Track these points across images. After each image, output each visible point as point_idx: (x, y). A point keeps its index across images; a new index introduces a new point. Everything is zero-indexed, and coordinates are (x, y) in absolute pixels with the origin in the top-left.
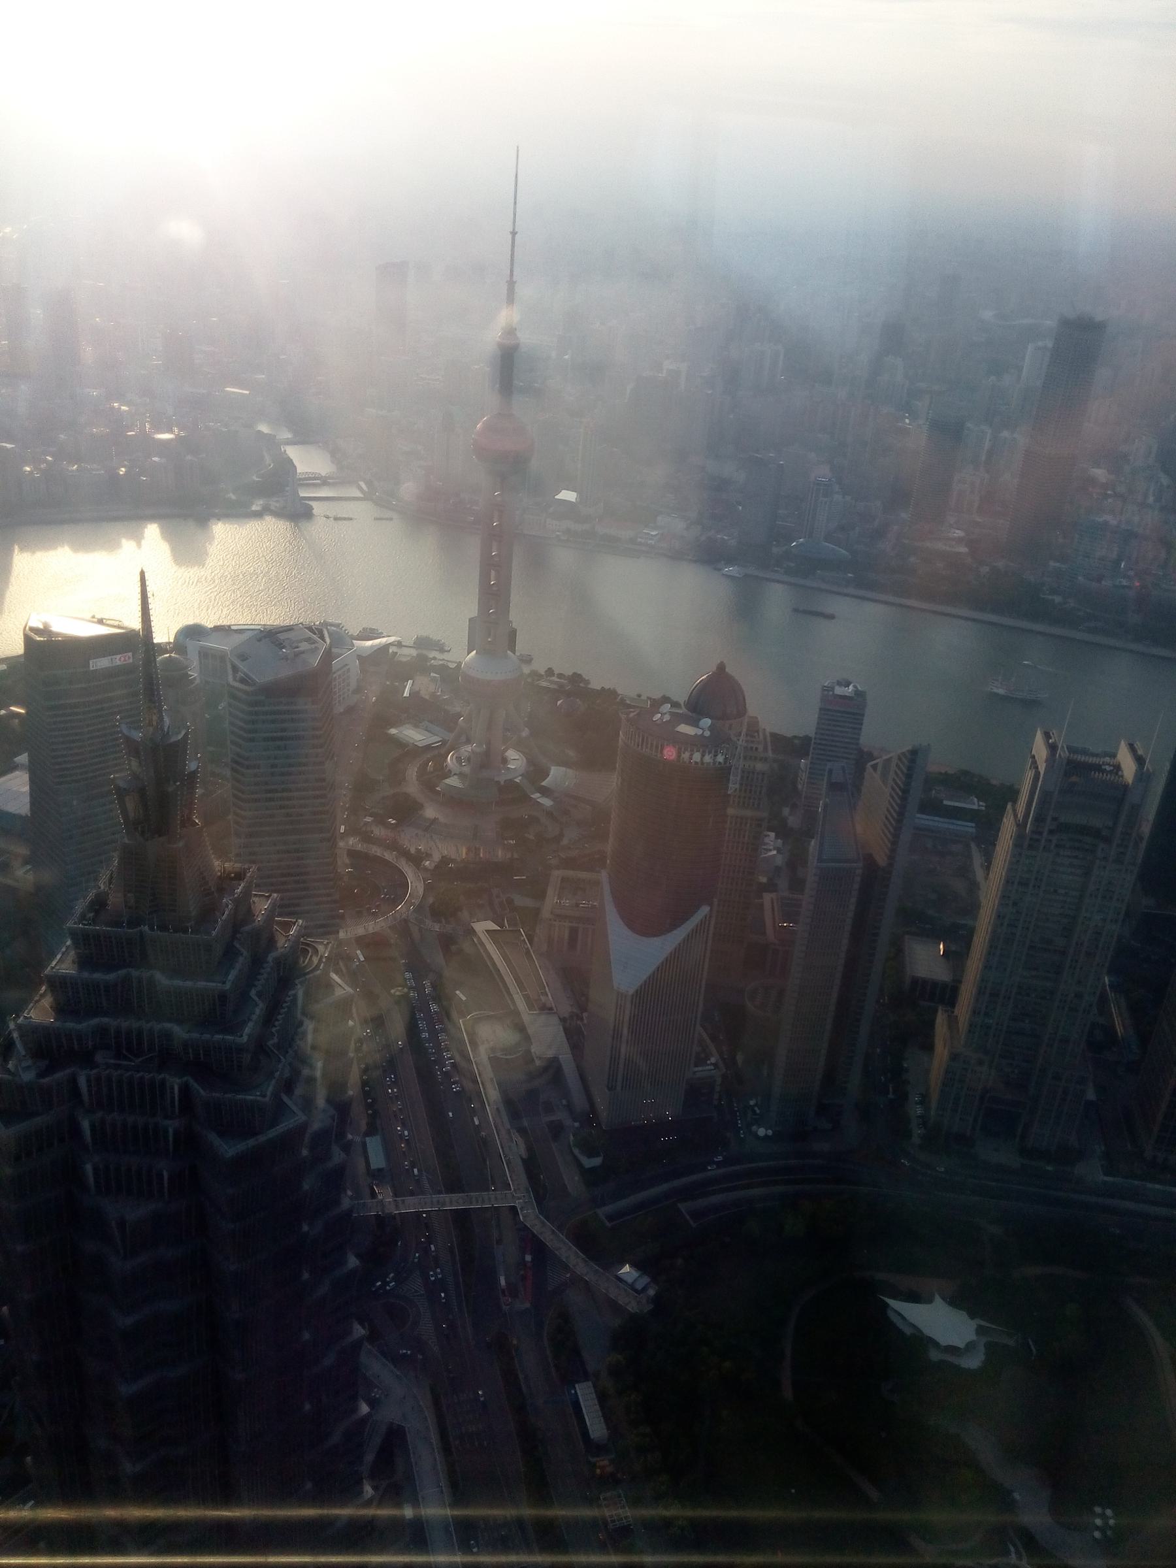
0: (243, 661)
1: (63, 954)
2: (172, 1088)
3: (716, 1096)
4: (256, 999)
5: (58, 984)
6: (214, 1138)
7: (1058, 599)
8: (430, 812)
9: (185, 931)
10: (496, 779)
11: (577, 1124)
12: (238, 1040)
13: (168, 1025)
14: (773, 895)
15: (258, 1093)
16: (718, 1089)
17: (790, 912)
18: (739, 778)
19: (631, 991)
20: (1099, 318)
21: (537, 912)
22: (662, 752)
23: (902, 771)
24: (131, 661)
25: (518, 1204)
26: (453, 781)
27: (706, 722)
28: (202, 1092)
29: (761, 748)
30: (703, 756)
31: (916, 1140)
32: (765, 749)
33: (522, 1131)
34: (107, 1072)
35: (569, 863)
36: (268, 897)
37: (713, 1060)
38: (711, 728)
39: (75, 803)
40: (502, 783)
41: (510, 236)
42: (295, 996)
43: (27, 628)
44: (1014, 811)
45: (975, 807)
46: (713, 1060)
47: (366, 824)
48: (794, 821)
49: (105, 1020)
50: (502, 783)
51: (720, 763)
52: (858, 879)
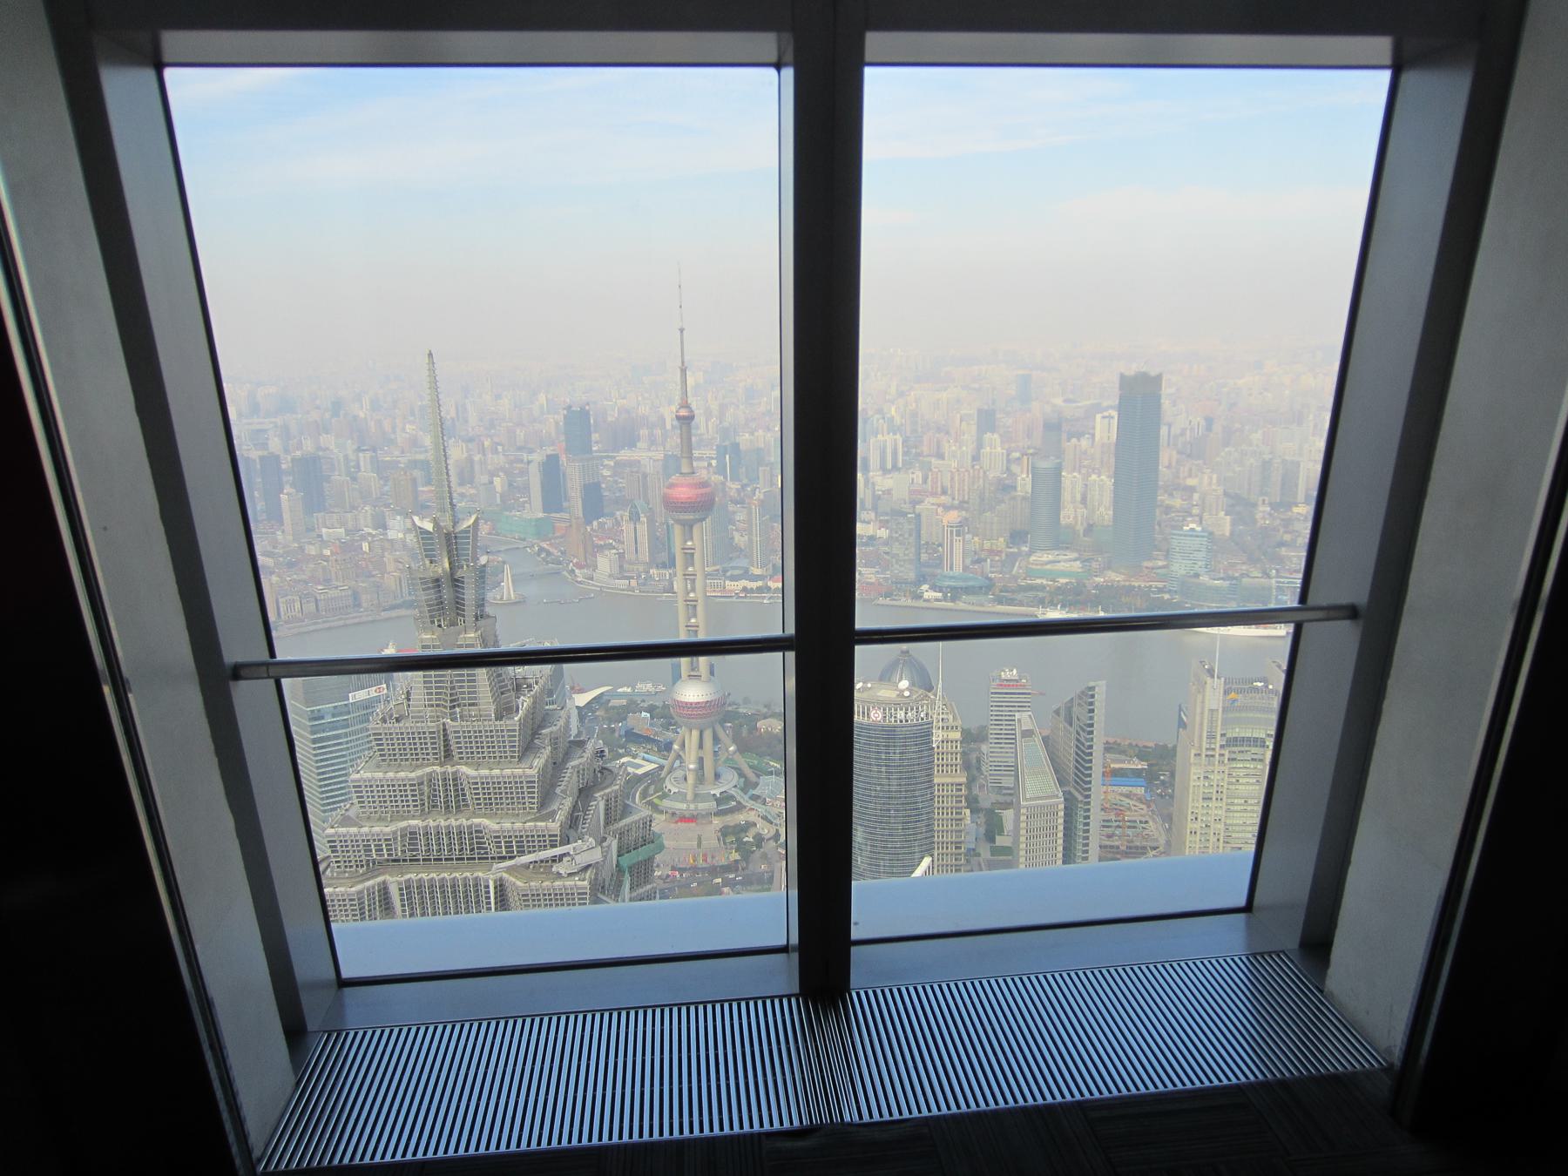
2: (487, 887)
7: (1167, 596)
10: (712, 792)
13: (476, 821)
15: (577, 878)
20: (1153, 373)
28: (519, 883)
29: (951, 717)
30: (906, 713)
40: (718, 795)
41: (679, 332)
45: (1140, 767)
48: (987, 799)
50: (718, 795)
51: (922, 719)
52: (1061, 814)
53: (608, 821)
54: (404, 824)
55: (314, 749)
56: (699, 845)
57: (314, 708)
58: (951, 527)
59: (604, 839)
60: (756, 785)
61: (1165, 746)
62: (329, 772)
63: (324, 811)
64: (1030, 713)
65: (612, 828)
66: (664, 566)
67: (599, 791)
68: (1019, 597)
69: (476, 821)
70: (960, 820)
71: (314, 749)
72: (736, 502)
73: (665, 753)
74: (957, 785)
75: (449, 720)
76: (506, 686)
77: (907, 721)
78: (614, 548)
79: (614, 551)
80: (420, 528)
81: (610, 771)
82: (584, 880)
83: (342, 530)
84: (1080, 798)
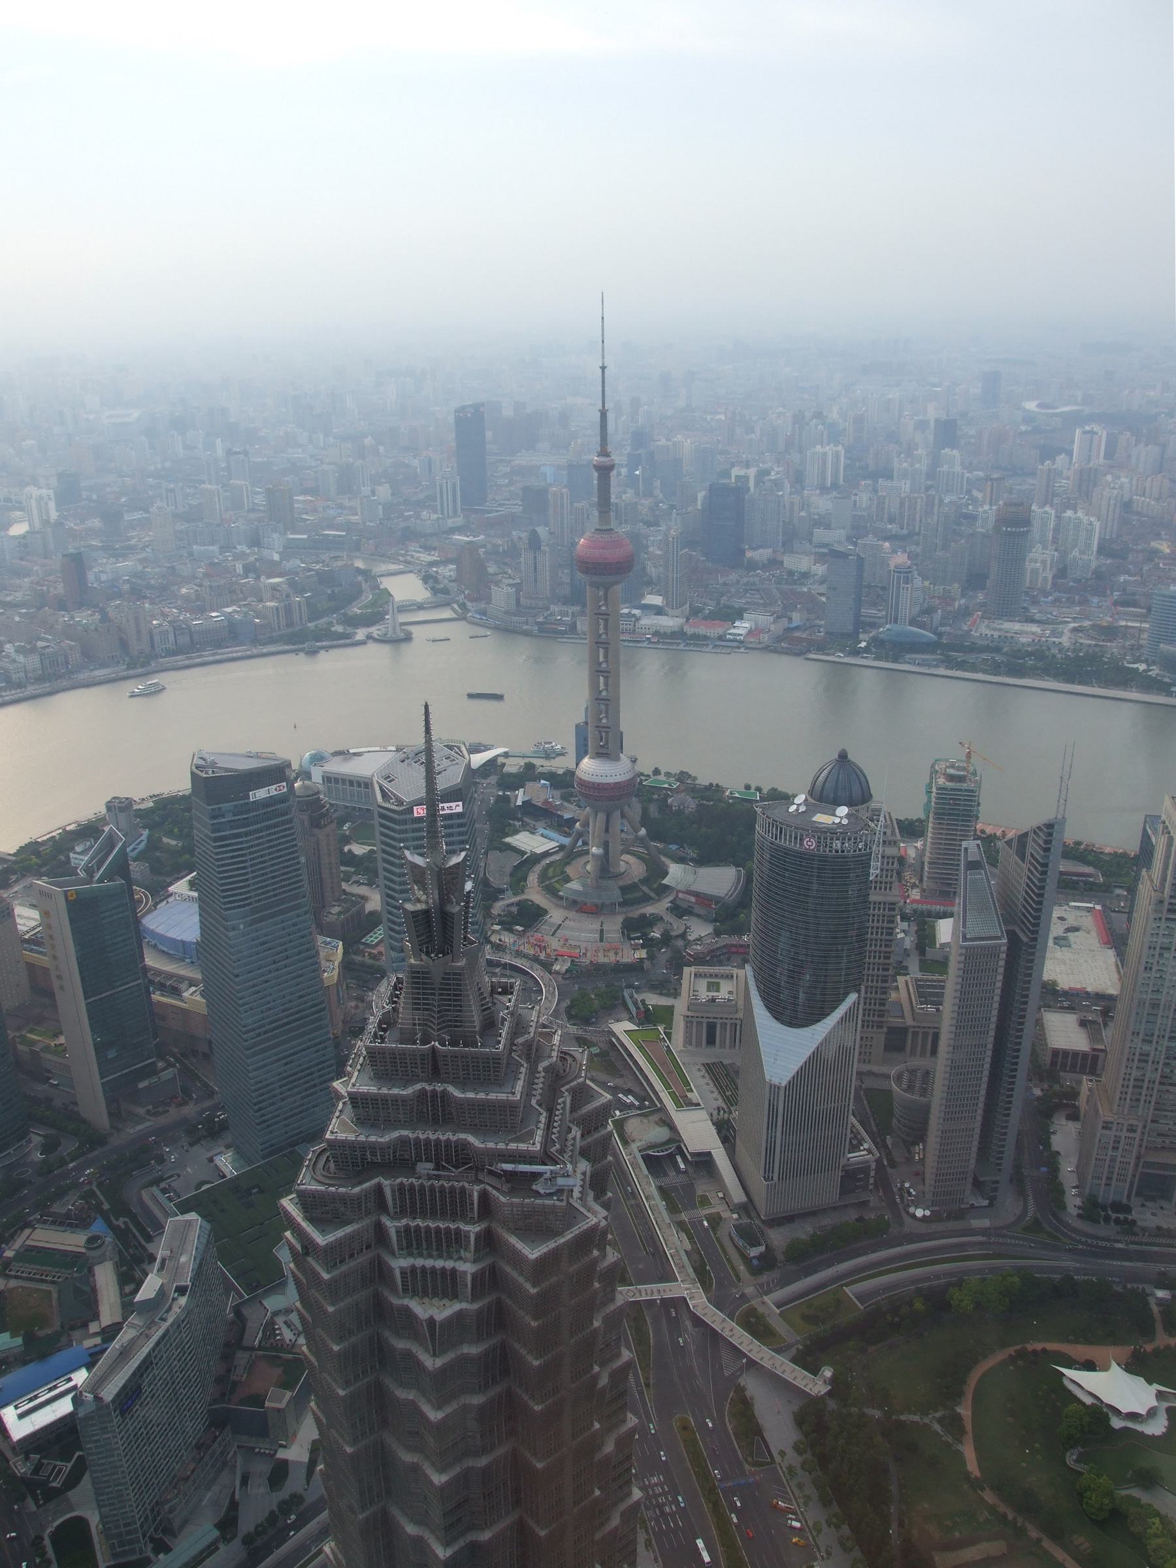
0: (390, 782)
1: (359, 1071)
2: (471, 1196)
3: (872, 1181)
4: (537, 1107)
5: (356, 1100)
6: (513, 1240)
8: (556, 915)
9: (474, 1045)
11: (735, 1216)
12: (531, 1148)
13: (462, 1136)
14: (908, 978)
15: (555, 1198)
16: (873, 1173)
17: (929, 994)
18: (879, 864)
19: (784, 1084)
21: (670, 1010)
22: (801, 844)
23: (1039, 845)
24: (285, 790)
25: (685, 1294)
26: (574, 885)
27: (843, 811)
28: (502, 1199)
30: (843, 843)
31: (1074, 1212)
32: (893, 833)
33: (681, 1226)
34: (430, 1182)
35: (699, 960)
36: (533, 1007)
37: (866, 1146)
38: (848, 816)
39: (242, 927)
42: (564, 1103)
43: (194, 767)
44: (1150, 877)
46: (866, 1146)
47: (494, 931)
49: (405, 1133)
51: (860, 850)
52: (1003, 956)
53: (573, 1110)
54: (395, 1134)
55: (216, 847)
56: (601, 940)
57: (216, 806)
58: (898, 572)
59: (569, 1130)
60: (665, 874)
61: (1124, 855)
62: (228, 858)
63: (226, 909)
64: (979, 842)
65: (576, 1115)
66: (566, 601)
67: (563, 1086)
68: (971, 658)
69: (462, 1136)
70: (891, 941)
71: (216, 847)
72: (649, 524)
73: (566, 829)
74: (890, 904)
75: (437, 1044)
76: (485, 998)
77: (842, 852)
78: (510, 577)
79: (511, 581)
80: (410, 862)
81: (573, 1057)
82: (562, 1200)
83: (215, 548)
84: (1025, 939)
